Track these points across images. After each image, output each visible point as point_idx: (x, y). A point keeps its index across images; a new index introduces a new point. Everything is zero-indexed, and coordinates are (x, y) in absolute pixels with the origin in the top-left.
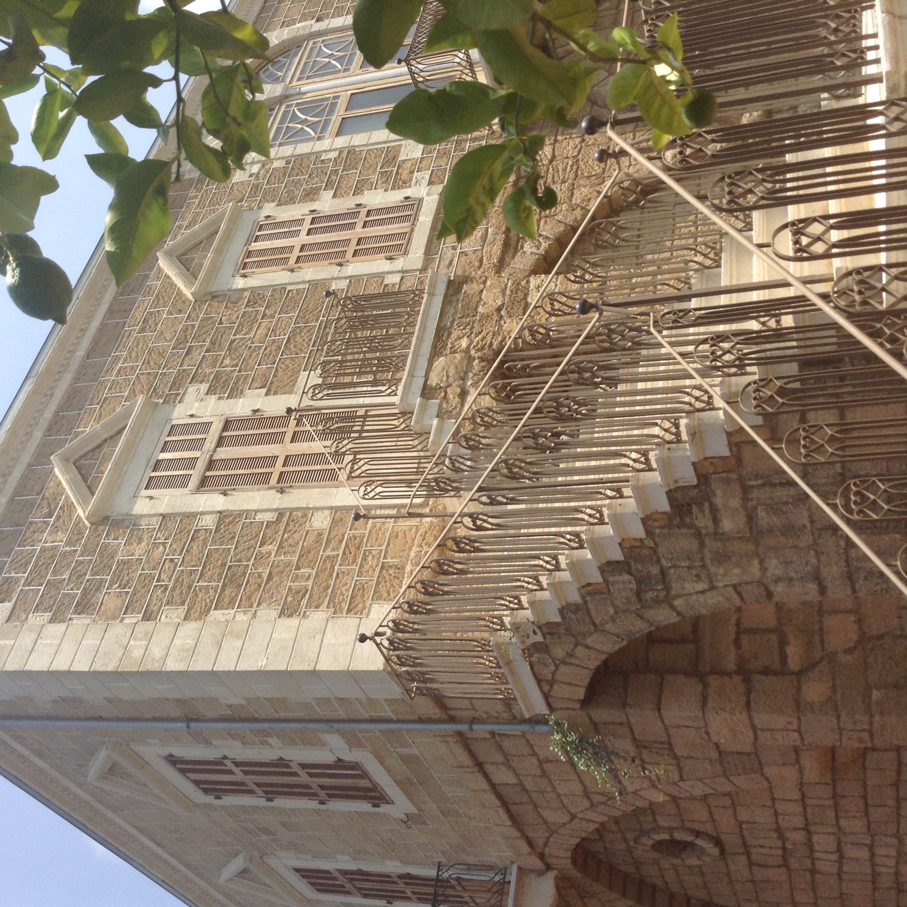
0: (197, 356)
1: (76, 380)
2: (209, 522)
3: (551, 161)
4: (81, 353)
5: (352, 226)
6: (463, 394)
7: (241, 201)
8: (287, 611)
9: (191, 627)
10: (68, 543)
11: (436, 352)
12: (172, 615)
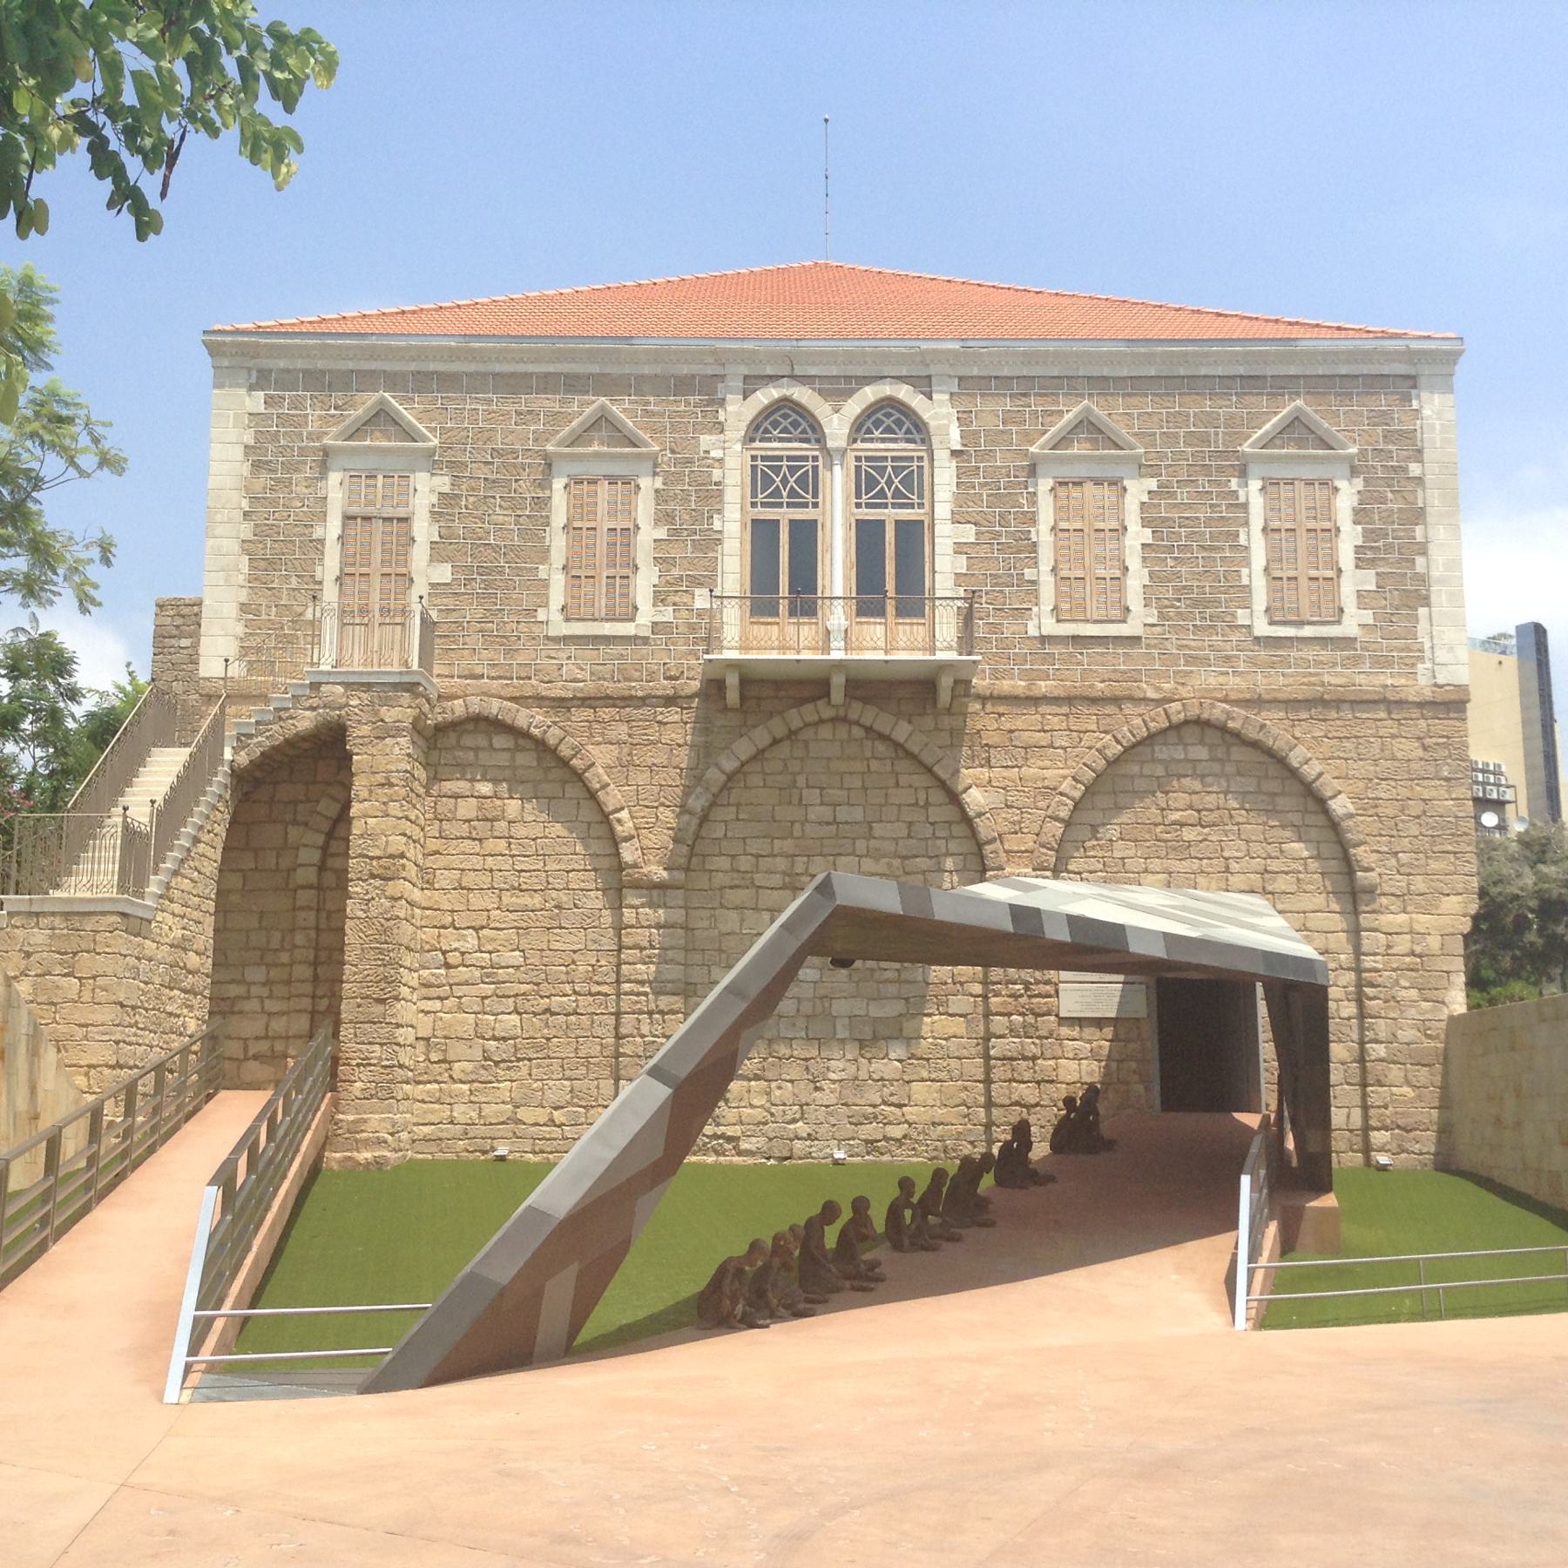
1: (469, 375)
2: (318, 533)
3: (659, 722)
4: (498, 368)
6: (313, 709)
7: (673, 452)
8: (244, 608)
9: (235, 547)
10: (310, 433)
11: (347, 685)
12: (246, 530)
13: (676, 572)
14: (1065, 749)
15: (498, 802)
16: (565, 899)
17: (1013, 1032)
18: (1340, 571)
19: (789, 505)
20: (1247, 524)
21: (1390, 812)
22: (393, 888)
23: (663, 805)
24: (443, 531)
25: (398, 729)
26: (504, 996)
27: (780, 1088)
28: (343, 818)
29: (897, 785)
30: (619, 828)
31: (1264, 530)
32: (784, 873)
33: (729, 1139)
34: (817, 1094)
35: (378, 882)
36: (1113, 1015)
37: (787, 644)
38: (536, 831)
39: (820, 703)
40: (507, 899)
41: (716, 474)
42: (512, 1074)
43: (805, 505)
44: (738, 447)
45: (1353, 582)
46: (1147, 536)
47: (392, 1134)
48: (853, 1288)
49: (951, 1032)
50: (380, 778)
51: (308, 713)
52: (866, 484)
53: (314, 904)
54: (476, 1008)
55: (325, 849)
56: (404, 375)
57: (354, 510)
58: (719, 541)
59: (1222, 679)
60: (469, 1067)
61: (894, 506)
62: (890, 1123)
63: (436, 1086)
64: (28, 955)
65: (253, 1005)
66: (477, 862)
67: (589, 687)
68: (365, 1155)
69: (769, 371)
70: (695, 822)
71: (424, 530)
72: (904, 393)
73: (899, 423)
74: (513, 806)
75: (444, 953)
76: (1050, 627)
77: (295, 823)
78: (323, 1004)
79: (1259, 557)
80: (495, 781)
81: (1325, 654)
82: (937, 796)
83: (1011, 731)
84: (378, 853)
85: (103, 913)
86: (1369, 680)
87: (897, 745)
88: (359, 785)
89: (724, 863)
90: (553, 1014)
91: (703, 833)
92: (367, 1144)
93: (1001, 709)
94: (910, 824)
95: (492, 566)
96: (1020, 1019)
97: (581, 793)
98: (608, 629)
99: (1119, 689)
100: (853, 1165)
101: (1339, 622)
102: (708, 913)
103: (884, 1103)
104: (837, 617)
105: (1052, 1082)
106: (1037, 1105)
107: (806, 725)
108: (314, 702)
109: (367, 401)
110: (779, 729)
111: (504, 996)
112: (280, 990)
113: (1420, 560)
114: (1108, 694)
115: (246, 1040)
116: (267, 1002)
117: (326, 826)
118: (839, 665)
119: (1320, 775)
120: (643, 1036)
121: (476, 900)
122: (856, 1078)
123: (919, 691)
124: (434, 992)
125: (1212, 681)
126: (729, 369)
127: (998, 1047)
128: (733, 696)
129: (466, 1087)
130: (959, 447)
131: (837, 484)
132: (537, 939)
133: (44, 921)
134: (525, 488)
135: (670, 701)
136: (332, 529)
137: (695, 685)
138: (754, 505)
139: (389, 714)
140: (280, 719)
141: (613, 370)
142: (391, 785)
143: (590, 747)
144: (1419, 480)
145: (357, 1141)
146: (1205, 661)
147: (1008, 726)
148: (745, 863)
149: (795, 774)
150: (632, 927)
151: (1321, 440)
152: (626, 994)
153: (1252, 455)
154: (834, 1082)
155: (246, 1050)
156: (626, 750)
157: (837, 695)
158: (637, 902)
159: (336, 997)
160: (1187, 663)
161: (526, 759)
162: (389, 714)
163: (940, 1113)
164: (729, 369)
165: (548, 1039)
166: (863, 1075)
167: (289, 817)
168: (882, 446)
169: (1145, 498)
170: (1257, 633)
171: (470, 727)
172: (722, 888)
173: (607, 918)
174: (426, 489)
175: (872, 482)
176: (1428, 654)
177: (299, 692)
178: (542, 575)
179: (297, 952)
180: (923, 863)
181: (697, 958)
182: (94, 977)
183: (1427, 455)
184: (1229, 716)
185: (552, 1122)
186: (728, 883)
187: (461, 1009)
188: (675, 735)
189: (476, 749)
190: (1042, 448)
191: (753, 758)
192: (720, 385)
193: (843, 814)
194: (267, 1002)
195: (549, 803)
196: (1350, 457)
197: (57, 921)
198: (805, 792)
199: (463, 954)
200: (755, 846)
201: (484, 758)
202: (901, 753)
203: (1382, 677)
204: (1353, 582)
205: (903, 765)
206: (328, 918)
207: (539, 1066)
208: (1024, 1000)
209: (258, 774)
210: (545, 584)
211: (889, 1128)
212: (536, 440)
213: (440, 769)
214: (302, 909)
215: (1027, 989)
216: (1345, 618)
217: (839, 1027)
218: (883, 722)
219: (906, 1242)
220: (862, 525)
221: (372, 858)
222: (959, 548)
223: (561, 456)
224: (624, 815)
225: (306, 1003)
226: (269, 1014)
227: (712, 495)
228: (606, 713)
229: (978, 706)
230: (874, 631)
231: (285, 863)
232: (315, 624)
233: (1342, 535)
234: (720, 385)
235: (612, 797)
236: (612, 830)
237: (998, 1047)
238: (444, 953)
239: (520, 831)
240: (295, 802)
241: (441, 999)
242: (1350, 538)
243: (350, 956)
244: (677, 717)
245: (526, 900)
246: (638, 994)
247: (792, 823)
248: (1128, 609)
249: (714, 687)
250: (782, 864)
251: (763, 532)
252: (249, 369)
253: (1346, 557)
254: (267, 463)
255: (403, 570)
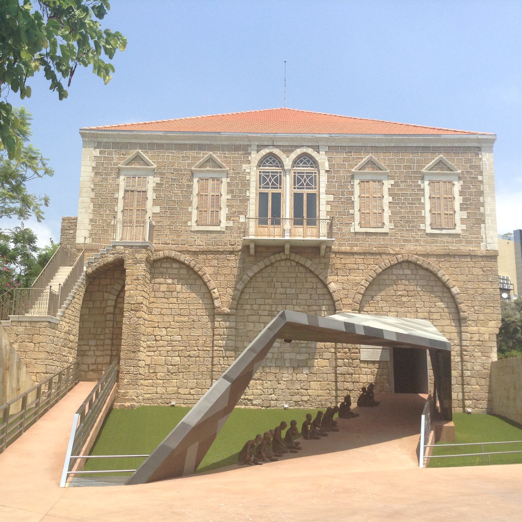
0: (171, 176)
2: (116, 196)
3: (228, 260)
4: (176, 142)
5: (213, 206)
6: (113, 254)
7: (233, 170)
8: (91, 220)
9: (89, 200)
10: (114, 163)
11: (125, 246)
12: (92, 195)
13: (234, 210)
14: (363, 270)
15: (174, 286)
16: (195, 318)
17: (345, 365)
18: (455, 212)
19: (272, 188)
20: (424, 196)
21: (472, 292)
22: (139, 314)
23: (228, 287)
24: (157, 195)
25: (141, 261)
26: (175, 351)
27: (266, 383)
28: (122, 290)
29: (307, 281)
30: (214, 295)
31: (430, 198)
32: (269, 311)
33: (249, 400)
34: (279, 385)
35: (133, 312)
36: (378, 360)
37: (270, 234)
38: (186, 295)
39: (281, 254)
40: (176, 318)
41: (248, 177)
42: (177, 377)
43: (277, 188)
44: (255, 168)
45: (459, 215)
46: (390, 199)
47: (137, 397)
48: (291, 452)
49: (324, 365)
50: (135, 277)
51: (111, 255)
52: (297, 181)
53: (112, 319)
54: (165, 355)
55: (116, 301)
56: (145, 144)
57: (128, 188)
58: (248, 200)
59: (415, 247)
60: (163, 374)
61: (306, 188)
62: (303, 395)
63: (152, 381)
64: (17, 335)
65: (92, 353)
66: (166, 306)
67: (205, 248)
68: (128, 404)
69: (265, 144)
70: (239, 293)
71: (151, 195)
72: (310, 151)
73: (308, 161)
74: (179, 287)
75: (155, 336)
76: (358, 229)
77: (106, 292)
78: (115, 353)
79: (428, 207)
80: (173, 279)
81: (450, 239)
82: (320, 285)
83: (345, 264)
84: (134, 302)
85: (42, 322)
86: (465, 248)
87: (307, 268)
88: (128, 280)
89: (249, 307)
90: (191, 357)
91: (242, 297)
92: (128, 400)
93: (341, 257)
94: (311, 295)
95: (173, 208)
96: (347, 361)
97: (202, 283)
98: (211, 228)
99: (381, 250)
100: (291, 409)
101: (454, 229)
102: (243, 324)
103: (301, 388)
104: (287, 225)
105: (358, 382)
106: (353, 390)
107: (276, 261)
108: (114, 252)
109: (133, 153)
110: (267, 262)
111: (175, 351)
112: (101, 348)
113: (482, 208)
114: (377, 252)
115: (89, 365)
116: (96, 352)
117: (117, 293)
118: (288, 241)
119: (448, 280)
120: (221, 365)
121: (166, 319)
122: (292, 380)
123: (315, 250)
124: (151, 349)
125: (412, 248)
126: (252, 143)
127: (340, 370)
128: (252, 251)
129: (161, 381)
130: (328, 169)
131: (288, 181)
132: (186, 332)
133: (23, 324)
134: (185, 182)
135: (231, 253)
136: (121, 194)
137: (240, 247)
138: (260, 188)
139: (138, 256)
140: (102, 257)
141: (214, 143)
142: (139, 280)
143: (204, 268)
144: (481, 182)
145: (125, 399)
146: (410, 241)
147: (344, 262)
148: (256, 307)
149: (272, 277)
150: (218, 328)
151: (449, 168)
152: (216, 350)
153: (426, 173)
154: (285, 381)
155: (89, 368)
156: (216, 269)
157: (287, 251)
158: (220, 320)
159: (119, 351)
160: (404, 242)
161: (184, 271)
162: (138, 256)
163: (320, 392)
164: (252, 143)
165: (189, 366)
166: (294, 379)
167: (105, 290)
168: (303, 168)
169: (390, 187)
170: (427, 232)
171: (165, 260)
172: (248, 315)
173: (209, 325)
174: (152, 181)
175: (299, 181)
176: (484, 239)
177: (109, 248)
178: (190, 210)
179: (106, 335)
180: (315, 308)
181: (239, 339)
182: (39, 343)
183: (484, 174)
184: (418, 260)
185: (190, 394)
186: (250, 314)
187: (160, 355)
188: (233, 264)
189: (167, 268)
190: (356, 170)
191: (259, 272)
192: (249, 148)
193: (288, 291)
194: (96, 352)
195: (191, 286)
196: (458, 174)
197: (27, 324)
198: (276, 283)
199: (161, 336)
200: (259, 301)
201: (170, 271)
202: (308, 270)
203: (469, 247)
204: (459, 215)
205: (309, 275)
206: (117, 323)
207: (186, 375)
208: (349, 354)
209: (95, 276)
210: (191, 213)
211: (303, 397)
212: (188, 166)
213: (155, 275)
214: (108, 321)
215: (349, 351)
216: (457, 228)
217: (286, 362)
218: (302, 261)
219: (309, 436)
220: (296, 195)
221: (132, 304)
222: (328, 203)
223: (196, 171)
224: (216, 290)
225: (109, 352)
226: (97, 356)
227: (246, 185)
228: (210, 256)
229: (334, 256)
230: (300, 230)
231: (103, 305)
232: (114, 226)
233: (456, 200)
234: (249, 148)
235: (212, 284)
236: (211, 295)
237: (340, 370)
238: (155, 336)
239: (181, 295)
240: (107, 285)
241: (154, 351)
242: (458, 201)
243: (124, 337)
244: (234, 258)
245: (183, 319)
246: (220, 351)
247: (272, 294)
248: (384, 224)
249: (246, 248)
250: (268, 307)
251: (263, 197)
252: (95, 142)
253: (457, 207)
254: (100, 173)
255: (144, 208)
